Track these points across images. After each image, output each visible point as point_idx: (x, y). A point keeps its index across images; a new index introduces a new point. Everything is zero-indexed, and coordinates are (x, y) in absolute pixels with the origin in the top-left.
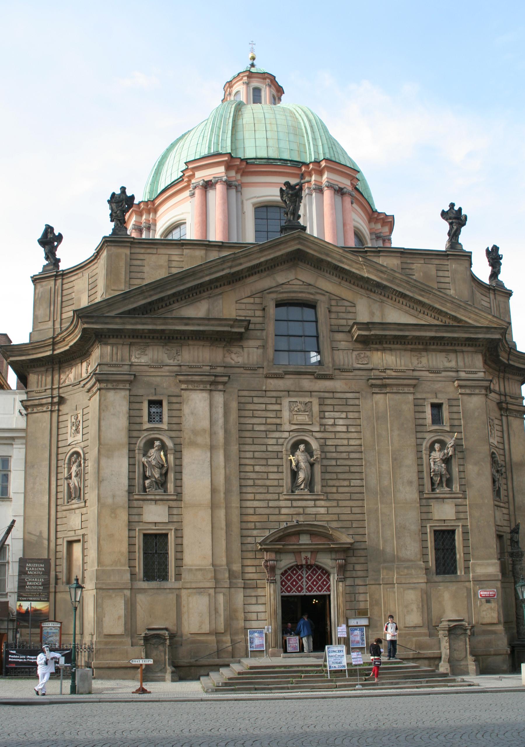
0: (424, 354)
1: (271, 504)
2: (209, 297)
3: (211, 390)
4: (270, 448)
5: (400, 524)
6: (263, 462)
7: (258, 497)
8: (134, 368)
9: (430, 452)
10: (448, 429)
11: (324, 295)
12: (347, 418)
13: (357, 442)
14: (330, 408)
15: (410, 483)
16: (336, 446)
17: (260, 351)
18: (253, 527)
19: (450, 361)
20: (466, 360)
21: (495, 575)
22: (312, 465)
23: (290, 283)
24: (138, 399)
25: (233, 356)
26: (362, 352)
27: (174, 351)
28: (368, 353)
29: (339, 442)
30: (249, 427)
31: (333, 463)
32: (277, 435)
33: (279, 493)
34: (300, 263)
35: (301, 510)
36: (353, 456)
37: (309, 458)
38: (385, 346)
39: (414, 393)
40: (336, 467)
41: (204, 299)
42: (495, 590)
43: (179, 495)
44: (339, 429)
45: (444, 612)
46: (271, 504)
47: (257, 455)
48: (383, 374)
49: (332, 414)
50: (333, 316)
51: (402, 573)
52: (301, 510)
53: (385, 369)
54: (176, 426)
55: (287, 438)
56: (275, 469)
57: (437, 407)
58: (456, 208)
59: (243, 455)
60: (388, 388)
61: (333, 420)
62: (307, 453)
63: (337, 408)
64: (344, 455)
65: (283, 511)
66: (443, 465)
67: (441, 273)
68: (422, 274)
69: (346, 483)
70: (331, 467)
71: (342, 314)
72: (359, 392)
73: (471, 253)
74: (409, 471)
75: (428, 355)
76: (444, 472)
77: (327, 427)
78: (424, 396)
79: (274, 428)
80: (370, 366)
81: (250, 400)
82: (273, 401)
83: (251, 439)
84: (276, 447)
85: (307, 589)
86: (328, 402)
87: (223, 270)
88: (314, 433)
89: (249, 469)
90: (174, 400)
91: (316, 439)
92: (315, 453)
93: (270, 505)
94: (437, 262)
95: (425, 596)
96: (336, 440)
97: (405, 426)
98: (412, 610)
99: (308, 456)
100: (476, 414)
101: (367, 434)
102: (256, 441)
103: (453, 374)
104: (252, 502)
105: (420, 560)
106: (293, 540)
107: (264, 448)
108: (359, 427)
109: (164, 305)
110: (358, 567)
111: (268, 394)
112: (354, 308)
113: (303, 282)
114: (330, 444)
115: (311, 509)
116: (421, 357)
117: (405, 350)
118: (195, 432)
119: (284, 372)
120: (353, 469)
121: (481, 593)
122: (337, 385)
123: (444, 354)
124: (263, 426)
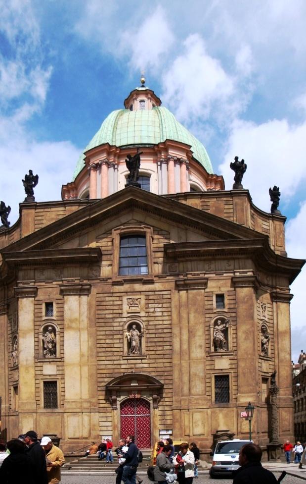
0: (213, 262)
1: (116, 362)
6: (111, 337)
9: (215, 326)
10: (226, 310)
11: (150, 228)
12: (162, 307)
13: (169, 322)
14: (152, 301)
15: (201, 346)
16: (155, 325)
17: (110, 267)
19: (230, 266)
20: (241, 264)
22: (140, 337)
23: (130, 222)
24: (40, 302)
27: (59, 272)
28: (177, 264)
31: (153, 336)
32: (119, 320)
33: (120, 356)
35: (133, 366)
36: (165, 331)
38: (187, 258)
40: (155, 339)
41: (76, 237)
43: (62, 360)
45: (219, 426)
46: (116, 362)
50: (155, 241)
51: (193, 403)
52: (133, 366)
54: (61, 317)
55: (125, 320)
56: (118, 341)
57: (220, 297)
58: (240, 160)
59: (99, 333)
61: (153, 309)
62: (137, 331)
65: (123, 366)
66: (222, 334)
67: (226, 207)
68: (214, 208)
69: (160, 348)
70: (152, 339)
71: (161, 240)
72: (170, 290)
73: (248, 190)
74: (200, 339)
75: (215, 263)
76: (222, 338)
78: (211, 290)
80: (177, 272)
81: (103, 299)
82: (117, 299)
85: (137, 413)
86: (151, 297)
88: (142, 318)
89: (102, 341)
90: (59, 301)
91: (143, 321)
92: (142, 330)
94: (225, 199)
96: (155, 322)
97: (198, 310)
98: (198, 425)
99: (138, 332)
100: (246, 300)
101: (175, 316)
102: (107, 324)
103: (232, 275)
105: (205, 395)
107: (111, 328)
110: (167, 399)
111: (115, 295)
112: (169, 235)
113: (137, 221)
116: (210, 264)
117: (201, 260)
118: (71, 321)
119: (124, 280)
122: (157, 286)
123: (226, 261)
124: (111, 315)
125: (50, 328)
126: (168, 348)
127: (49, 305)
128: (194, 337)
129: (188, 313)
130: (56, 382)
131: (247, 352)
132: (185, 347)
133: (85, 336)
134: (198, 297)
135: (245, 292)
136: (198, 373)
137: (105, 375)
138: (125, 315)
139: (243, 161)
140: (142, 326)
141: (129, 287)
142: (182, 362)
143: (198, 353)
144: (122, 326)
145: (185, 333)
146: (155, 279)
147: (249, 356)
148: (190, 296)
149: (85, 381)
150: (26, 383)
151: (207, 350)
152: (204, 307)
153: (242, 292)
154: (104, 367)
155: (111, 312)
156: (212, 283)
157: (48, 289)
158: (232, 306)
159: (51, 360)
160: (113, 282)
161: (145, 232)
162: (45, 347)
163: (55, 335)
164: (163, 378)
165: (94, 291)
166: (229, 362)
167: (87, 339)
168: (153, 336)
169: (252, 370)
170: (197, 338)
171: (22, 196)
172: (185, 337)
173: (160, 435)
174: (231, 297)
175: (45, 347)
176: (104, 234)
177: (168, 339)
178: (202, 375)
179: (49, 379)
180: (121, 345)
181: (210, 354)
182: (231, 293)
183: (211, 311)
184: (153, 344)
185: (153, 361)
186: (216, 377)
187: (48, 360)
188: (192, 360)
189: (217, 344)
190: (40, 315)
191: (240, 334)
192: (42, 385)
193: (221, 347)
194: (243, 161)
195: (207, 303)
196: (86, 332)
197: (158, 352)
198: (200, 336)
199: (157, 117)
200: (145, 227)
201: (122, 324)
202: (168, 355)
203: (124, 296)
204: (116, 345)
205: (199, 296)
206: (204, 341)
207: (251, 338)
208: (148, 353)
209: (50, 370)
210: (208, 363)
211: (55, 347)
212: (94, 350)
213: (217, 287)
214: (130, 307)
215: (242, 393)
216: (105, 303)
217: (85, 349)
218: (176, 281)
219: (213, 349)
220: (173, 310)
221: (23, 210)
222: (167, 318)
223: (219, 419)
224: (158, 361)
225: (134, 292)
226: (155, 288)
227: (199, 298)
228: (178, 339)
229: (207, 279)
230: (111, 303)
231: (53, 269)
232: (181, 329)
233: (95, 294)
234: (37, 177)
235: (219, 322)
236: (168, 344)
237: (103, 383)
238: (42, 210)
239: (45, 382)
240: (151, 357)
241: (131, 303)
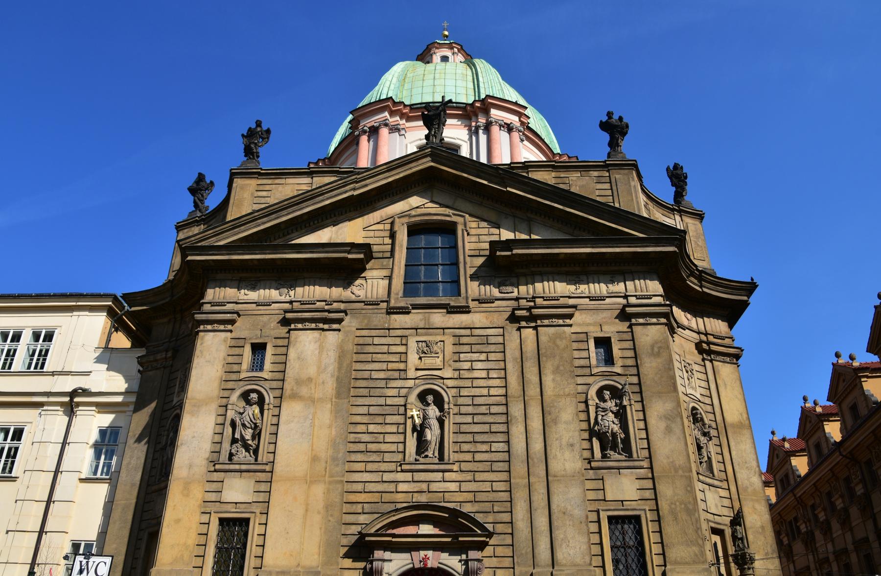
5: (558, 506)
6: (380, 419)
7: (370, 467)
10: (617, 369)
13: (502, 391)
14: (467, 348)
18: (360, 511)
29: (477, 392)
30: (366, 374)
31: (469, 419)
32: (399, 383)
35: (424, 487)
36: (494, 409)
37: (438, 414)
38: (533, 269)
39: (571, 326)
44: (476, 374)
47: (373, 410)
48: (532, 304)
49: (469, 356)
56: (393, 429)
57: (604, 343)
58: (616, 117)
61: (469, 363)
63: (475, 348)
64: (483, 409)
65: (402, 487)
66: (616, 420)
69: (485, 447)
70: (465, 426)
74: (568, 430)
76: (616, 428)
82: (398, 341)
83: (368, 390)
84: (396, 399)
86: (464, 340)
87: (346, 192)
90: (280, 342)
92: (446, 406)
93: (384, 479)
94: (596, 174)
97: (562, 368)
99: (437, 410)
100: (656, 350)
104: (361, 474)
106: (411, 530)
107: (382, 401)
108: (503, 372)
109: (281, 235)
114: (466, 394)
115: (437, 484)
118: (299, 382)
119: (411, 305)
120: (494, 428)
122: (475, 318)
125: (254, 396)
126: (502, 447)
127: (259, 349)
128: (555, 421)
130: (247, 521)
131: (672, 462)
132: (537, 446)
133: (325, 415)
134: (558, 342)
135: (650, 334)
136: (569, 507)
137: (360, 506)
138: (411, 373)
139: (621, 119)
140: (446, 399)
141: (421, 320)
144: (406, 397)
145: (535, 412)
146: (472, 304)
147: (680, 472)
148: (543, 339)
149: (317, 519)
150: (178, 521)
151: (587, 454)
152: (571, 362)
153: (647, 335)
154: (359, 487)
155: (384, 366)
156: (584, 316)
157: (260, 318)
158: (631, 362)
159: (244, 467)
161: (455, 224)
162: (237, 436)
163: (262, 412)
164: (490, 518)
165: (349, 322)
166: (638, 484)
167: (328, 422)
168: (469, 419)
169: (691, 507)
170: (561, 427)
171: (238, 158)
172: (536, 424)
175: (237, 436)
177: (503, 428)
178: (578, 513)
179: (232, 514)
180: (400, 438)
183: (587, 371)
184: (469, 438)
185: (469, 477)
186: (610, 519)
187: (237, 467)
188: (555, 476)
189: (607, 442)
190: (236, 368)
191: (652, 421)
192: (214, 529)
193: (614, 448)
194: (621, 119)
195: (576, 354)
196: (329, 406)
197: (478, 457)
198: (566, 423)
199: (469, 69)
200: (454, 214)
201: (403, 392)
202: (501, 464)
204: (389, 438)
205: (561, 339)
206: (577, 434)
209: (238, 491)
210: (590, 485)
211: (257, 435)
212: (341, 447)
213: (594, 324)
214: (420, 358)
215: (676, 563)
216: (371, 349)
217: (322, 446)
218: (514, 310)
219: (598, 454)
220: (510, 366)
221: (235, 180)
222: (497, 382)
224: (479, 476)
225: (429, 328)
227: (562, 344)
228: (522, 428)
229: (575, 307)
230: (385, 349)
231: (276, 281)
234: (268, 131)
235: (607, 394)
236: (501, 438)
237: (353, 527)
238: (270, 181)
239: (222, 521)
240: (464, 466)
241: (425, 349)
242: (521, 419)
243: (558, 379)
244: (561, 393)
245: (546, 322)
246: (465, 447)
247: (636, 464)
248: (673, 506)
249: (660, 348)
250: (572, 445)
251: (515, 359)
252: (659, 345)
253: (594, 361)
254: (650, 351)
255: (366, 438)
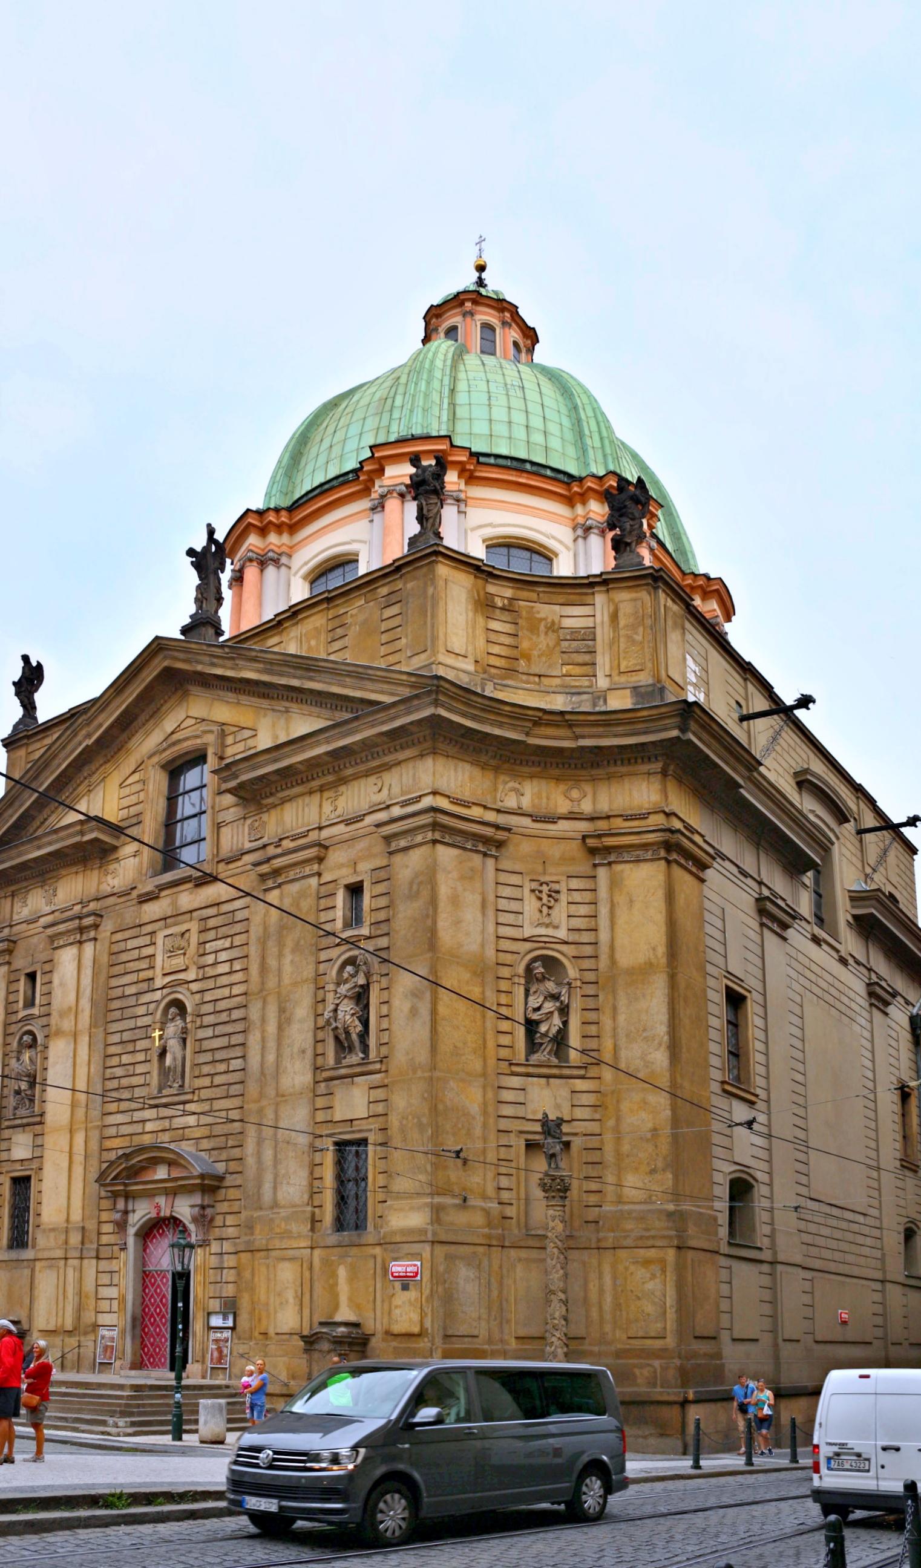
2: (89, 791)
3: (80, 942)
4: (141, 1022)
8: (16, 929)
11: (211, 732)
14: (212, 935)
21: (423, 1231)
25: (109, 877)
26: (257, 818)
30: (118, 992)
34: (191, 688)
42: (419, 1263)
45: (336, 1307)
53: (281, 840)
57: (355, 890)
60: (283, 876)
63: (223, 931)
64: (224, 1017)
65: (149, 1127)
69: (222, 1067)
74: (301, 1034)
77: (206, 969)
79: (144, 986)
86: (211, 923)
89: (115, 1061)
95: (307, 1274)
97: (302, 942)
98: (287, 1302)
100: (415, 887)
107: (131, 1024)
119: (157, 887)
121: (394, 1270)
128: (289, 1024)
129: (280, 956)
131: (412, 1059)
132: (271, 1058)
138: (159, 982)
140: (189, 1010)
142: (264, 1103)
143: (298, 1075)
153: (407, 867)
155: (133, 977)
156: (337, 854)
160: (139, 896)
164: (224, 1156)
169: (424, 1120)
172: (272, 1028)
173: (210, 1328)
174: (381, 888)
176: (134, 772)
181: (326, 1074)
182: (383, 874)
186: (336, 1144)
197: (218, 1080)
203: (160, 929)
207: (424, 1009)
208: (199, 1082)
210: (320, 1102)
216: (124, 957)
220: (253, 950)
223: (336, 1284)
226: (219, 895)
231: (42, 886)
232: (265, 1002)
233: (109, 934)
242: (258, 1024)
243: (297, 959)
244: (299, 980)
245: (292, 875)
246: (206, 1069)
247: (371, 1067)
248: (404, 1122)
249: (421, 883)
250: (303, 1052)
251: (259, 939)
252: (421, 878)
253: (339, 924)
254: (406, 892)
255: (119, 1072)
